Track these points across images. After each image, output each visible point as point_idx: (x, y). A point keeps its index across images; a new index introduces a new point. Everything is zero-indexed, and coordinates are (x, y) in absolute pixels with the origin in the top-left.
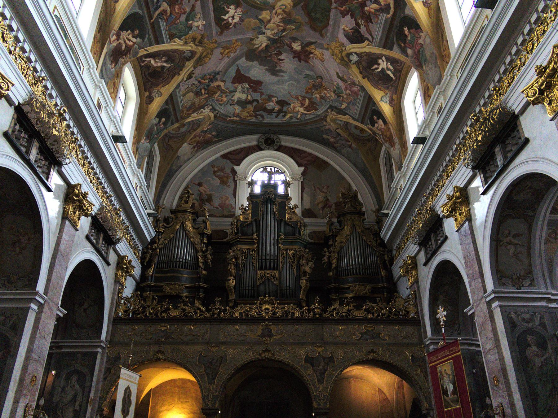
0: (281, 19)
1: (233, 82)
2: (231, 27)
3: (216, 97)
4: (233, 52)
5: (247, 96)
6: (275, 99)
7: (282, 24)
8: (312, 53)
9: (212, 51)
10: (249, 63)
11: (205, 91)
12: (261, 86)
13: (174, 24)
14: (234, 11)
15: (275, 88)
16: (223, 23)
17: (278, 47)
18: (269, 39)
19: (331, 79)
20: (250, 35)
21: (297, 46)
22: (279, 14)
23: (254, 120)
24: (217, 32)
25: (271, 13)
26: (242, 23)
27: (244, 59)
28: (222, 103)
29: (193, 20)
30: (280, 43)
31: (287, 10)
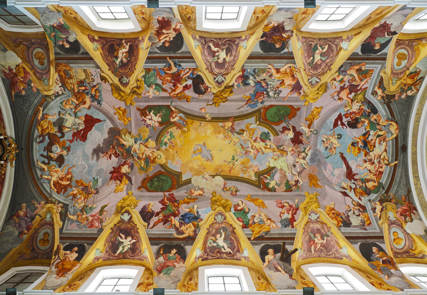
0: (149, 156)
1: (87, 116)
2: (143, 117)
3: (72, 99)
4: (120, 117)
5: (69, 128)
6: (65, 153)
7: (144, 156)
8: (121, 182)
9: (123, 100)
10: (106, 130)
11: (82, 90)
12: (81, 140)
13: (157, 74)
14: (156, 121)
15: (79, 153)
16: (147, 111)
17: (123, 154)
18: (130, 147)
19: (99, 201)
20: (134, 132)
21: (125, 169)
22: (153, 154)
23: (36, 133)
24: (139, 106)
25: (154, 148)
26: (145, 126)
27: (111, 126)
28: (64, 103)
29: (155, 89)
30: (127, 156)
31: (157, 160)
